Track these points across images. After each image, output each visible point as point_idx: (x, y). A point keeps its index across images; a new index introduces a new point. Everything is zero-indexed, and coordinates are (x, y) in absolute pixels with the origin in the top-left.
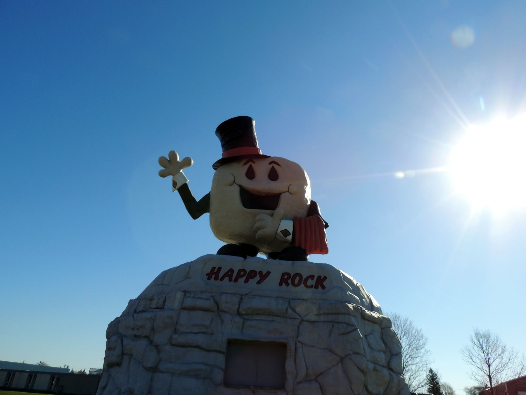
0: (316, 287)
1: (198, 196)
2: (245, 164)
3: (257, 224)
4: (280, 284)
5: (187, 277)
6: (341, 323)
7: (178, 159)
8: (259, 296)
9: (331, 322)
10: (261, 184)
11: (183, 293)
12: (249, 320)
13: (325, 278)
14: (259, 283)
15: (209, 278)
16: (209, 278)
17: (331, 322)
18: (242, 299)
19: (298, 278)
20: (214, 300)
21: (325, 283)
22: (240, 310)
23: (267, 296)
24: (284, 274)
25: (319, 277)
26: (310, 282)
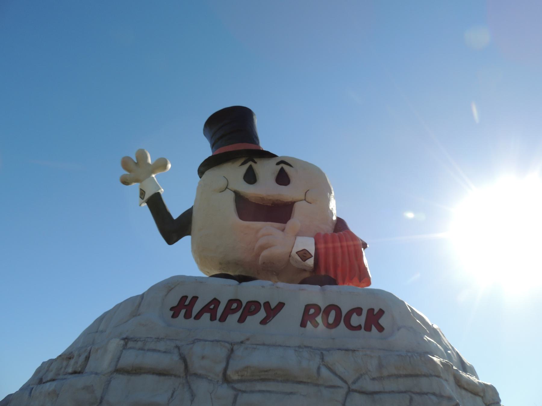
0: (368, 328)
1: (176, 211)
2: (243, 164)
3: (262, 241)
4: (303, 325)
5: (135, 314)
6: (427, 394)
7: (150, 161)
8: (264, 344)
9: (405, 392)
10: (266, 188)
11: (122, 342)
12: (244, 392)
13: (381, 312)
14: (264, 322)
16: (174, 316)
17: (405, 392)
18: (232, 351)
19: (333, 314)
20: (180, 354)
21: (382, 321)
22: (229, 372)
23: (280, 346)
24: (308, 307)
25: (371, 311)
26: (355, 320)
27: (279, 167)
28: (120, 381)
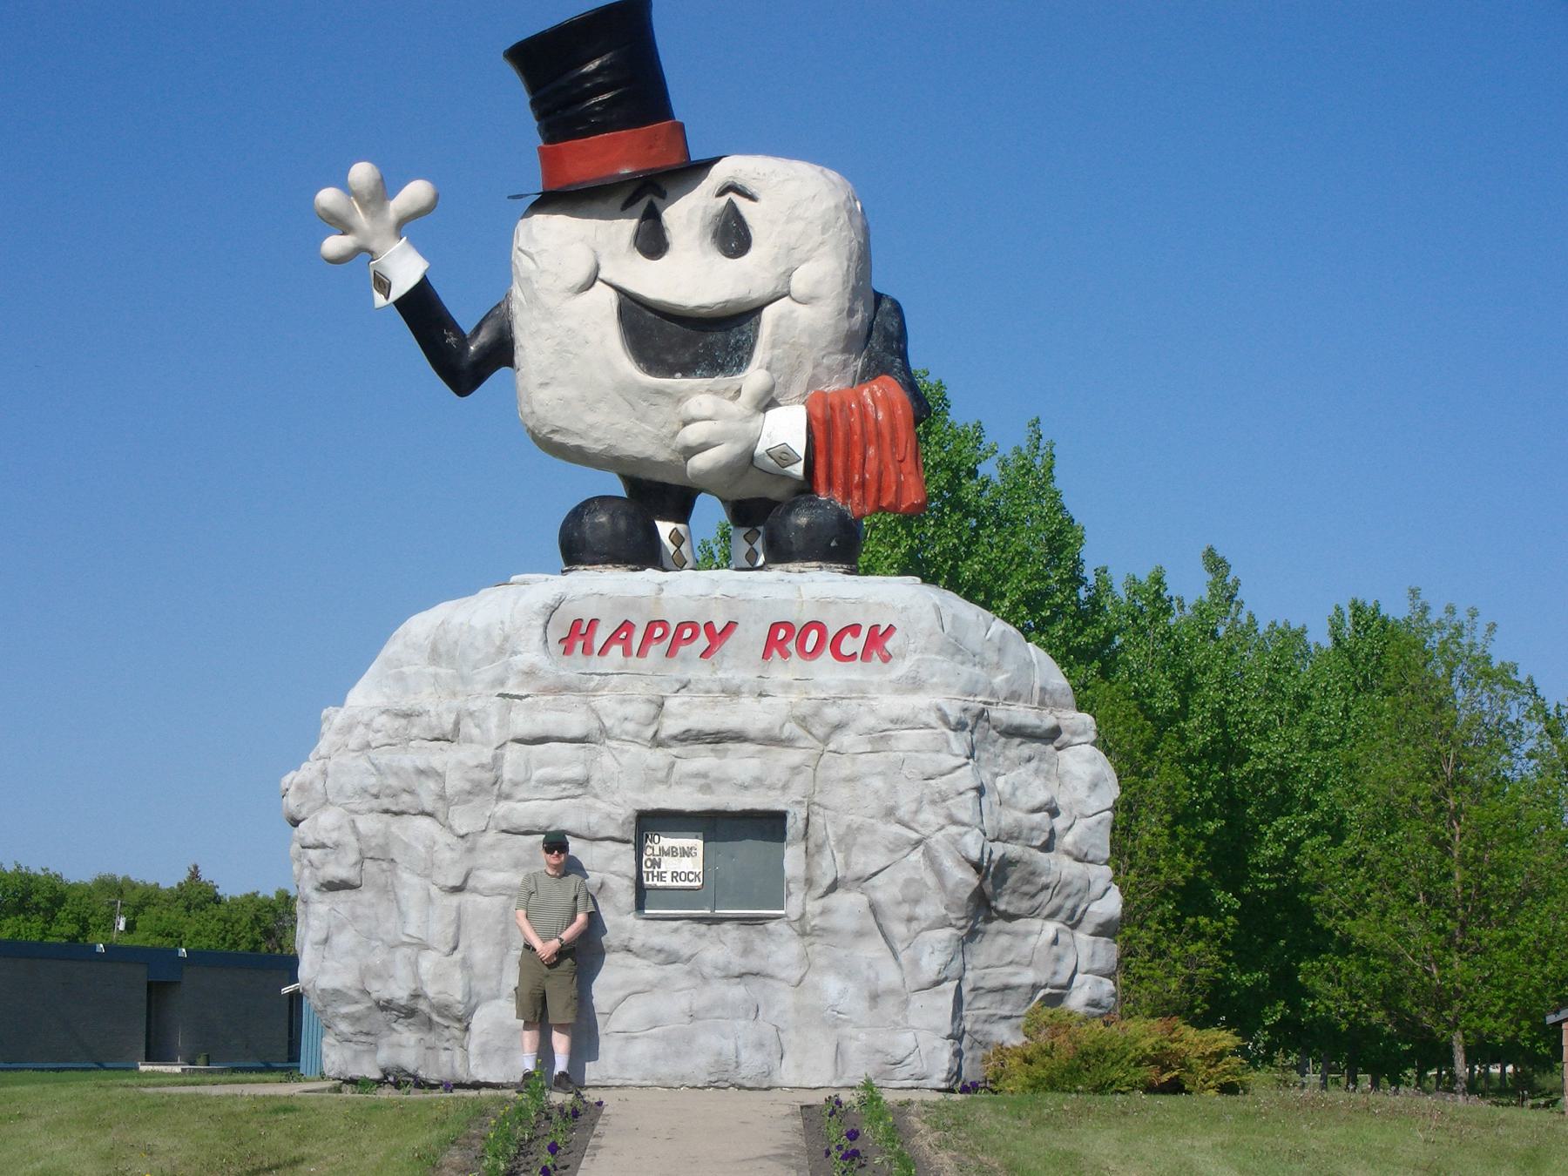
0: (866, 655)
4: (767, 654)
13: (891, 629)
14: (706, 654)
15: (568, 651)
16: (568, 651)
21: (889, 645)
24: (775, 627)
25: (874, 628)
26: (849, 645)
27: (724, 200)
28: (514, 753)
